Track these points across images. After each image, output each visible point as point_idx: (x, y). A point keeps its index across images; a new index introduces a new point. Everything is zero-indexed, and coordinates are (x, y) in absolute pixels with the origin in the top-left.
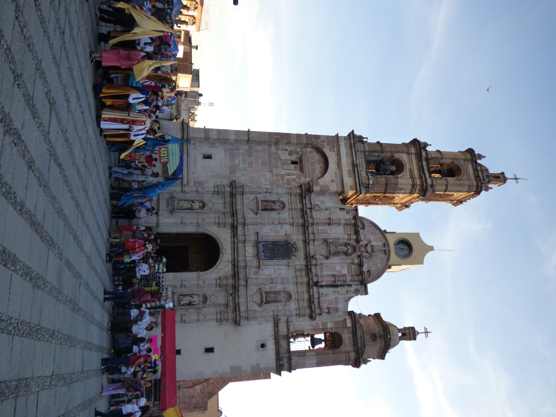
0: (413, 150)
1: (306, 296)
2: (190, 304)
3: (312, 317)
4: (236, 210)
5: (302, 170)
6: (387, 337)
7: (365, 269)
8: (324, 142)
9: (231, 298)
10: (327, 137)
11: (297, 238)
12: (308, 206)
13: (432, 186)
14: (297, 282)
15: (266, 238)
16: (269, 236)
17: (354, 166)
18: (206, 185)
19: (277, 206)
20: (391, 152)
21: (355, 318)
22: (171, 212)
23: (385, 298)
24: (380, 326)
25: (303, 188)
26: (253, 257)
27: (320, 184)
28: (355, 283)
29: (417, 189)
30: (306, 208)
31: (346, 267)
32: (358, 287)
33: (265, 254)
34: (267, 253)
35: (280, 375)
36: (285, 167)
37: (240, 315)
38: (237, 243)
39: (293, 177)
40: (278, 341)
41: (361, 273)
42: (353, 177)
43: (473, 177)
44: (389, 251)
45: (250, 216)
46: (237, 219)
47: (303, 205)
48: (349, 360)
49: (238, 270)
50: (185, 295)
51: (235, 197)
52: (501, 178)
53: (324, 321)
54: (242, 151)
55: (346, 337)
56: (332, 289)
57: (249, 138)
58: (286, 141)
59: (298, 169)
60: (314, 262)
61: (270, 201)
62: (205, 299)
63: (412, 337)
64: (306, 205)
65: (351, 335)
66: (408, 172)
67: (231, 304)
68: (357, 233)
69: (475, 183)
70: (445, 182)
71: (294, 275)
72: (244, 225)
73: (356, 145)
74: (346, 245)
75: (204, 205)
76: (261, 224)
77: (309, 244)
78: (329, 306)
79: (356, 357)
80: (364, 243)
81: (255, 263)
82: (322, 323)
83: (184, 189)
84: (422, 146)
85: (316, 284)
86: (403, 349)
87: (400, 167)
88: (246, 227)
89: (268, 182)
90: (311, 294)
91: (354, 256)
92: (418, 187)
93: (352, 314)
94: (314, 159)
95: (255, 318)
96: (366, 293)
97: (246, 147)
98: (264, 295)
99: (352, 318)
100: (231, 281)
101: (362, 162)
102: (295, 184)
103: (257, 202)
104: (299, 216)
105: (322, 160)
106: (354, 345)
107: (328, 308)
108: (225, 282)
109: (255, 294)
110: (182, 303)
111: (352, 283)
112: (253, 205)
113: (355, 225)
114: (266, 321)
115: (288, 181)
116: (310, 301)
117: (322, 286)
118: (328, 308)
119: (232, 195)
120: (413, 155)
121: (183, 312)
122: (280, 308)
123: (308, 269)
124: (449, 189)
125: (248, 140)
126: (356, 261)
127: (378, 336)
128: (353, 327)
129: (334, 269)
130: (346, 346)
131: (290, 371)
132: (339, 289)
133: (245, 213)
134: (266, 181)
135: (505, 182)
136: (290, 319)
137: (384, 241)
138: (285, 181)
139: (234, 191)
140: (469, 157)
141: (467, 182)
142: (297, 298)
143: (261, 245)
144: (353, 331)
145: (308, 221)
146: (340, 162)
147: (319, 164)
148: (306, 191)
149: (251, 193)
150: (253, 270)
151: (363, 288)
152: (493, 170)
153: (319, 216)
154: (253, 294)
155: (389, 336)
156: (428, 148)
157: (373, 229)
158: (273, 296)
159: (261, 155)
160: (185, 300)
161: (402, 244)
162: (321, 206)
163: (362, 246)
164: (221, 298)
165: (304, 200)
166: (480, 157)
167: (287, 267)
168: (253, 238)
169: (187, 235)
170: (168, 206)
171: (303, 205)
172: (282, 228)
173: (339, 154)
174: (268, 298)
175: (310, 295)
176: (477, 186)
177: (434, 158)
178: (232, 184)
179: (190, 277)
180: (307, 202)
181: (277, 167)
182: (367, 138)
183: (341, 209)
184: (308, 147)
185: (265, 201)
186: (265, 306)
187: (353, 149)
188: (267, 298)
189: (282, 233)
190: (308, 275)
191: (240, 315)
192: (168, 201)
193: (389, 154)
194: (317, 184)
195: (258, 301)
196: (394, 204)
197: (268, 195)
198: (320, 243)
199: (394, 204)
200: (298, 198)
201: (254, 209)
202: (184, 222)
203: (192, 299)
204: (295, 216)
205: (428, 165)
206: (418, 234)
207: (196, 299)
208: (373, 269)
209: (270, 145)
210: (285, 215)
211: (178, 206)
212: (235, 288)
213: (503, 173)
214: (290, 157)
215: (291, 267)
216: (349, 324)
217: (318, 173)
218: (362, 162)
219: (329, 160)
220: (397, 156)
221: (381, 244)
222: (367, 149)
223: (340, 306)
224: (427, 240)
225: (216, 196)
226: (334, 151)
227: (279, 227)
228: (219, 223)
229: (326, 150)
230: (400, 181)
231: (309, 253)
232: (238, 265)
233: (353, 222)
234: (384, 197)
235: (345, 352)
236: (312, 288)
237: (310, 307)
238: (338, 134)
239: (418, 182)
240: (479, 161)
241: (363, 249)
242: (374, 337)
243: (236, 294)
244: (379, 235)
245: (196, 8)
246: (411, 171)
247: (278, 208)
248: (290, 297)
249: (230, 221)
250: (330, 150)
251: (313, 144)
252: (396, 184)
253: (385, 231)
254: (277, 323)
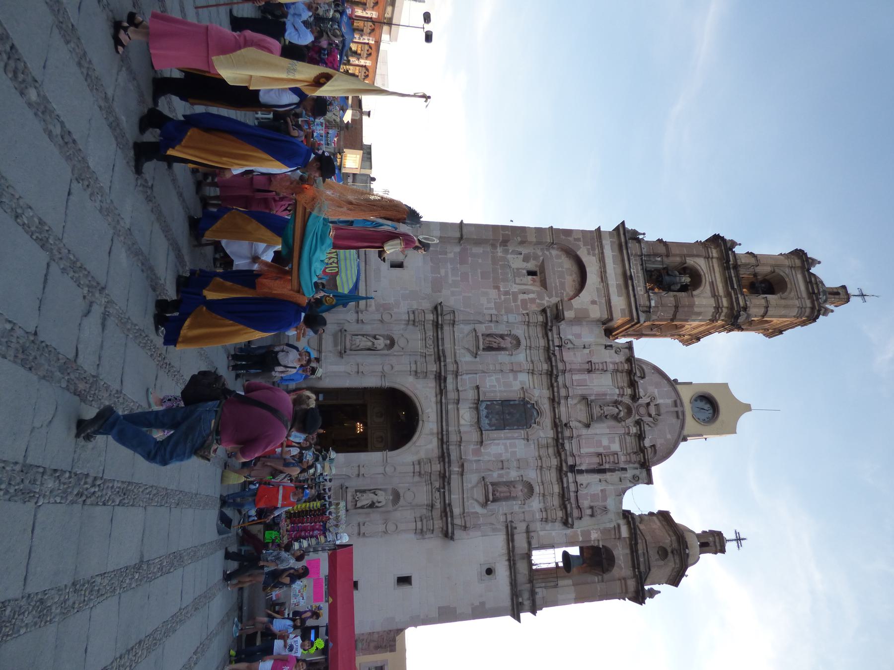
0: (714, 253)
1: (556, 489)
2: (372, 505)
3: (566, 523)
4: (443, 351)
5: (544, 284)
6: (685, 552)
7: (647, 443)
8: (578, 240)
9: (437, 495)
10: (583, 232)
11: (540, 394)
12: (557, 342)
13: (745, 309)
14: (541, 466)
15: (491, 396)
16: (495, 391)
17: (627, 278)
18: (395, 310)
19: (507, 343)
20: (681, 256)
21: (634, 523)
22: (341, 354)
23: (680, 487)
24: (671, 533)
25: (549, 314)
26: (471, 425)
27: (575, 306)
28: (631, 465)
29: (723, 314)
30: (554, 346)
31: (617, 439)
32: (637, 472)
33: (490, 420)
34: (494, 420)
35: (519, 620)
36: (518, 280)
37: (453, 524)
38: (447, 404)
39: (532, 296)
40: (514, 564)
41: (642, 450)
42: (625, 295)
43: (804, 295)
44: (683, 413)
45: (465, 358)
46: (445, 365)
47: (548, 340)
48: (627, 592)
49: (448, 449)
50: (364, 491)
51: (442, 329)
52: (841, 295)
53: (585, 529)
54: (451, 255)
55: (621, 553)
56: (597, 477)
57: (462, 235)
58: (519, 239)
59: (538, 283)
60: (567, 433)
61: (496, 335)
62: (396, 496)
63: (719, 548)
64: (553, 341)
65: (628, 551)
66: (708, 287)
67: (438, 505)
68: (633, 384)
69: (808, 303)
70: (763, 302)
71: (537, 454)
72: (456, 374)
73: (630, 245)
74: (616, 403)
75: (392, 343)
76: (484, 372)
77: (559, 403)
78: (592, 504)
79: (637, 587)
80: (644, 400)
81: (475, 436)
82: (583, 533)
83: (361, 316)
84: (729, 245)
85: (572, 468)
86: (704, 568)
87: (696, 280)
88: (459, 377)
89: (492, 305)
90: (565, 485)
91: (630, 421)
92: (725, 310)
93: (627, 515)
94: (562, 267)
95: (477, 527)
96: (650, 481)
97: (457, 249)
98: (490, 487)
99: (628, 523)
100: (437, 467)
101: (638, 273)
102: (534, 308)
103: (477, 337)
104: (542, 359)
105: (574, 268)
106: (634, 567)
107: (592, 508)
108: (427, 468)
109: (476, 486)
110: (359, 505)
111: (626, 466)
112: (470, 343)
113: (630, 373)
114: (495, 530)
115: (524, 302)
116: (563, 496)
117: (581, 472)
118: (592, 508)
119: (437, 326)
120: (715, 261)
121: (361, 519)
122: (516, 508)
123: (558, 445)
124: (769, 313)
125: (461, 238)
126: (634, 430)
127: (669, 550)
128: (630, 539)
129: (599, 443)
130: (621, 568)
131: (534, 612)
132: (608, 476)
133: (457, 355)
134: (488, 302)
135: (848, 300)
136: (532, 528)
137: (674, 396)
138: (519, 303)
139: (439, 319)
140: (798, 262)
141: (797, 303)
142: (542, 492)
143: (483, 405)
144: (631, 545)
145: (557, 366)
146: (605, 272)
147: (571, 275)
148: (553, 318)
149: (467, 322)
150: (472, 447)
151: (644, 474)
152: (830, 281)
153: (573, 358)
154: (473, 488)
155: (687, 551)
156: (737, 250)
157: (657, 378)
158: (504, 489)
159: (480, 261)
160: (365, 500)
161: (701, 401)
162: (577, 342)
163: (641, 405)
164: (422, 494)
165: (550, 334)
167: (526, 442)
168: (471, 395)
169: (365, 390)
170: (336, 345)
171: (548, 340)
172: (515, 379)
173: (602, 260)
174: (498, 494)
175: (563, 488)
176: (813, 308)
177: (746, 265)
178: (437, 309)
179: (371, 460)
180: (555, 336)
181: (505, 280)
182: (644, 234)
183: (606, 347)
184: (553, 248)
185: (488, 335)
186: (492, 506)
187: (625, 252)
188: (494, 494)
189: (516, 386)
190: (558, 454)
191: (453, 524)
192: (335, 336)
193: (678, 259)
194: (571, 308)
195: (482, 499)
196: (680, 335)
197: (492, 325)
198: (575, 401)
199: (680, 335)
200: (539, 329)
201: (471, 349)
202: (360, 370)
203: (375, 498)
204: (535, 359)
205: (737, 276)
206: (725, 386)
207: (382, 497)
208: (659, 443)
209: (494, 246)
210: (521, 357)
211: (352, 345)
212: (444, 477)
213: (844, 287)
214: (525, 265)
215: (531, 442)
216: (625, 532)
217: (569, 290)
218: (638, 273)
219: (588, 270)
220: (690, 261)
221: (669, 401)
222: (645, 251)
223: (610, 503)
224: (740, 394)
225: (411, 327)
226: (594, 255)
227: (511, 377)
228: (416, 372)
229: (583, 253)
230: (697, 301)
231: (559, 418)
232: (448, 441)
233: (626, 366)
234: (671, 327)
235: (620, 580)
236: (566, 476)
237: (564, 507)
238: (599, 228)
239: (725, 302)
240: (813, 270)
241: (643, 410)
242: (663, 553)
243: (446, 488)
244: (667, 388)
245: (370, 54)
247: (509, 345)
248: (530, 489)
249: (433, 368)
250: (589, 254)
251: (561, 241)
252: (692, 306)
253: (676, 381)
254: (512, 535)
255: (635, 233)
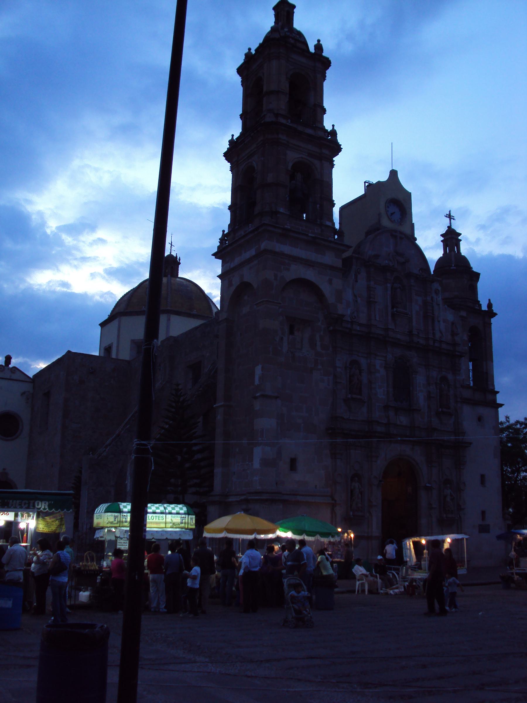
216: (463, 313)
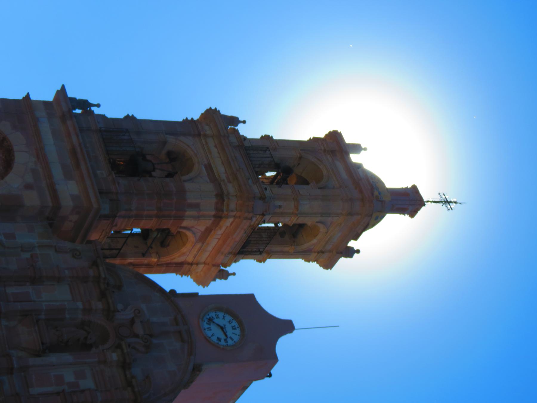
126: (114, 356)
166: (357, 148)
182: (98, 106)
246: (209, 167)
255: (85, 104)
